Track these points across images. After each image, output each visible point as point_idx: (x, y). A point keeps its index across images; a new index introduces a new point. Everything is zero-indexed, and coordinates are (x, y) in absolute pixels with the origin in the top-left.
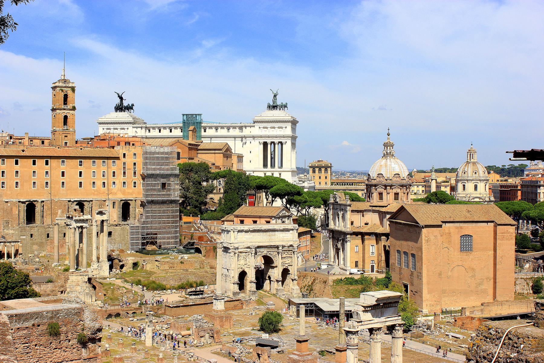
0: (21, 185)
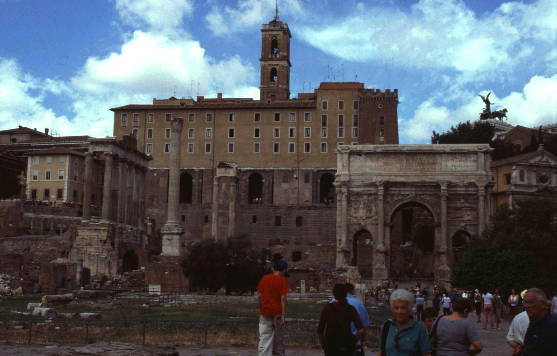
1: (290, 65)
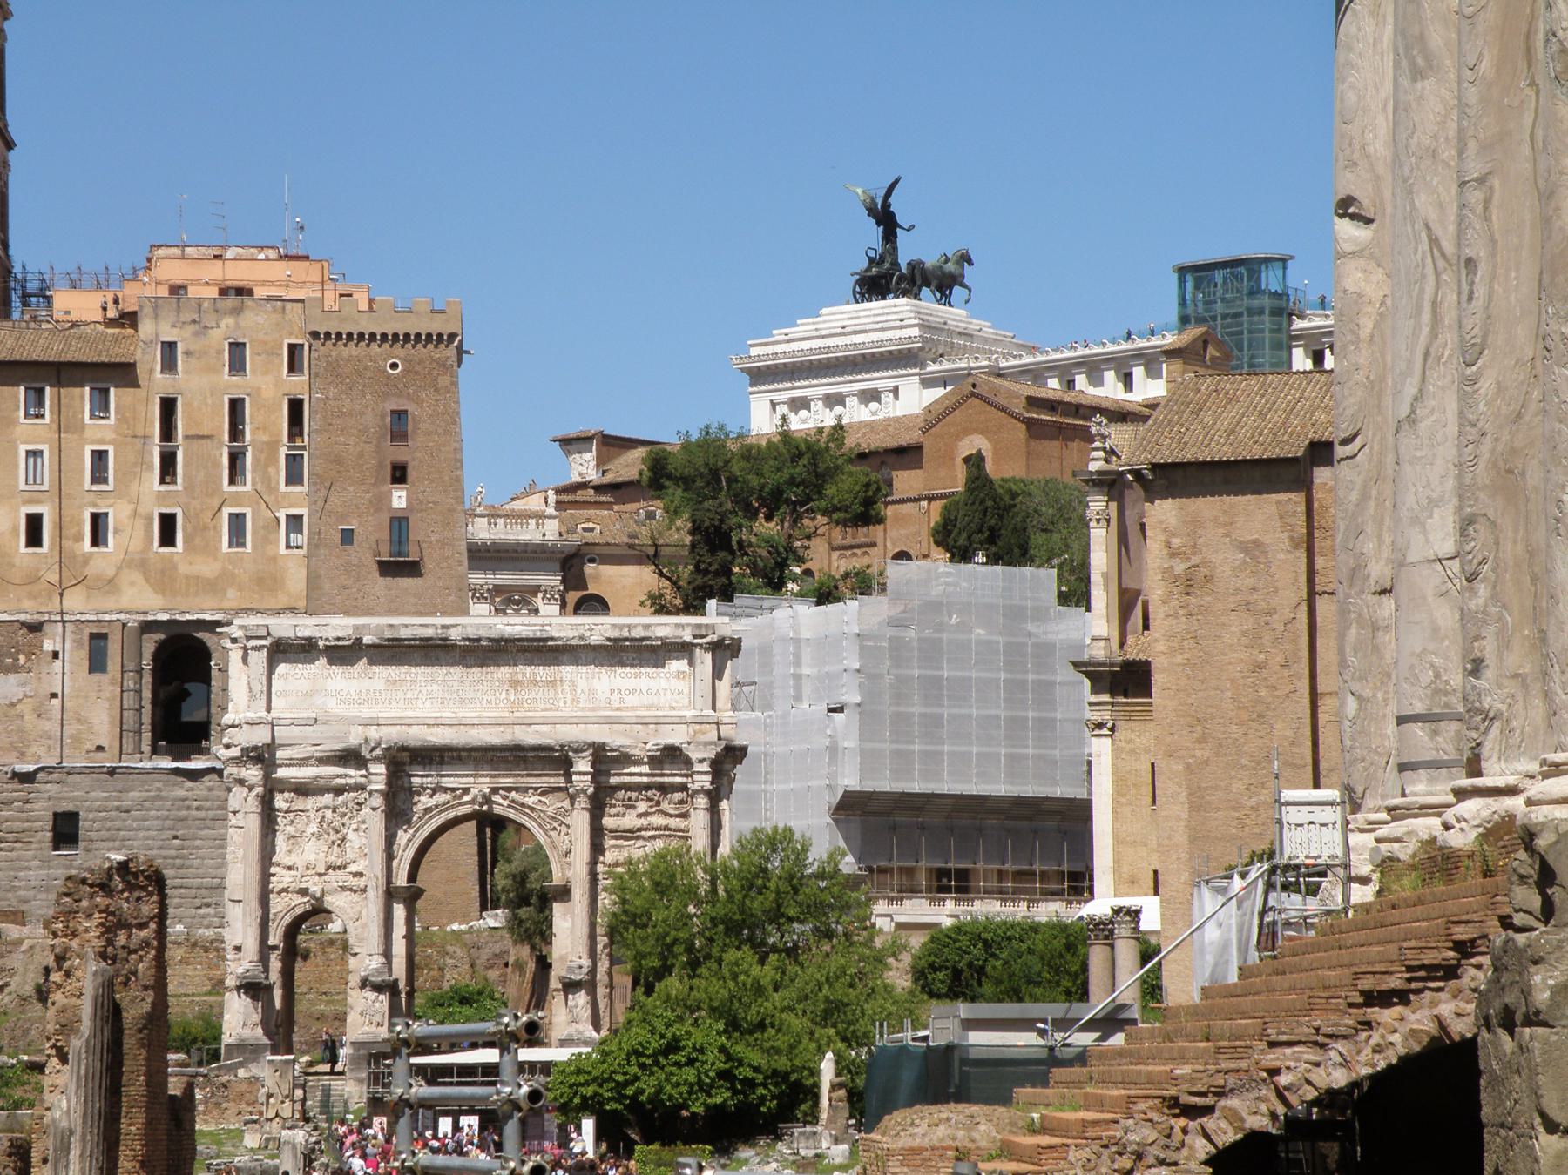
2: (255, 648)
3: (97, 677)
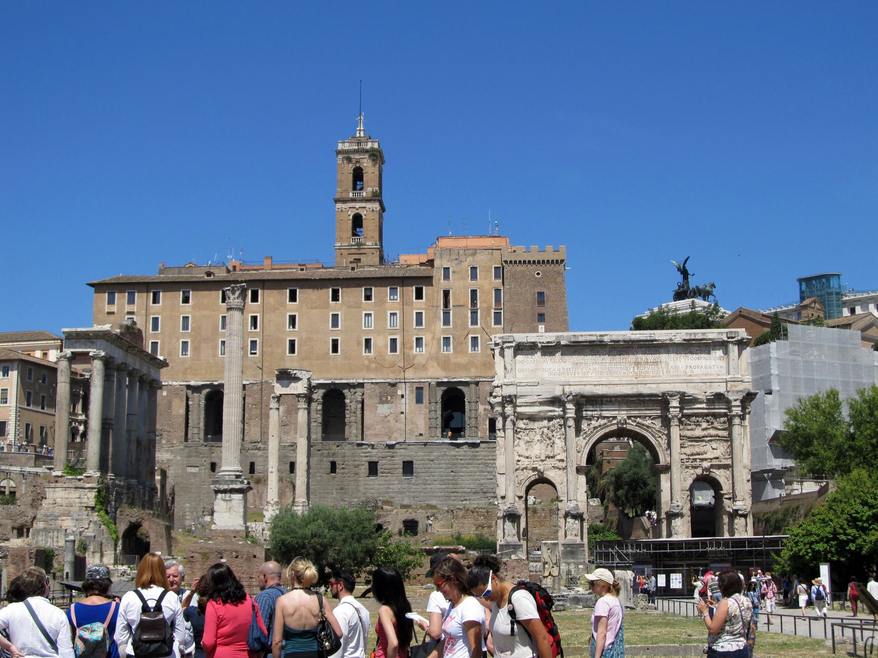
0: (196, 349)
1: (383, 209)
2: (509, 347)
3: (419, 405)
